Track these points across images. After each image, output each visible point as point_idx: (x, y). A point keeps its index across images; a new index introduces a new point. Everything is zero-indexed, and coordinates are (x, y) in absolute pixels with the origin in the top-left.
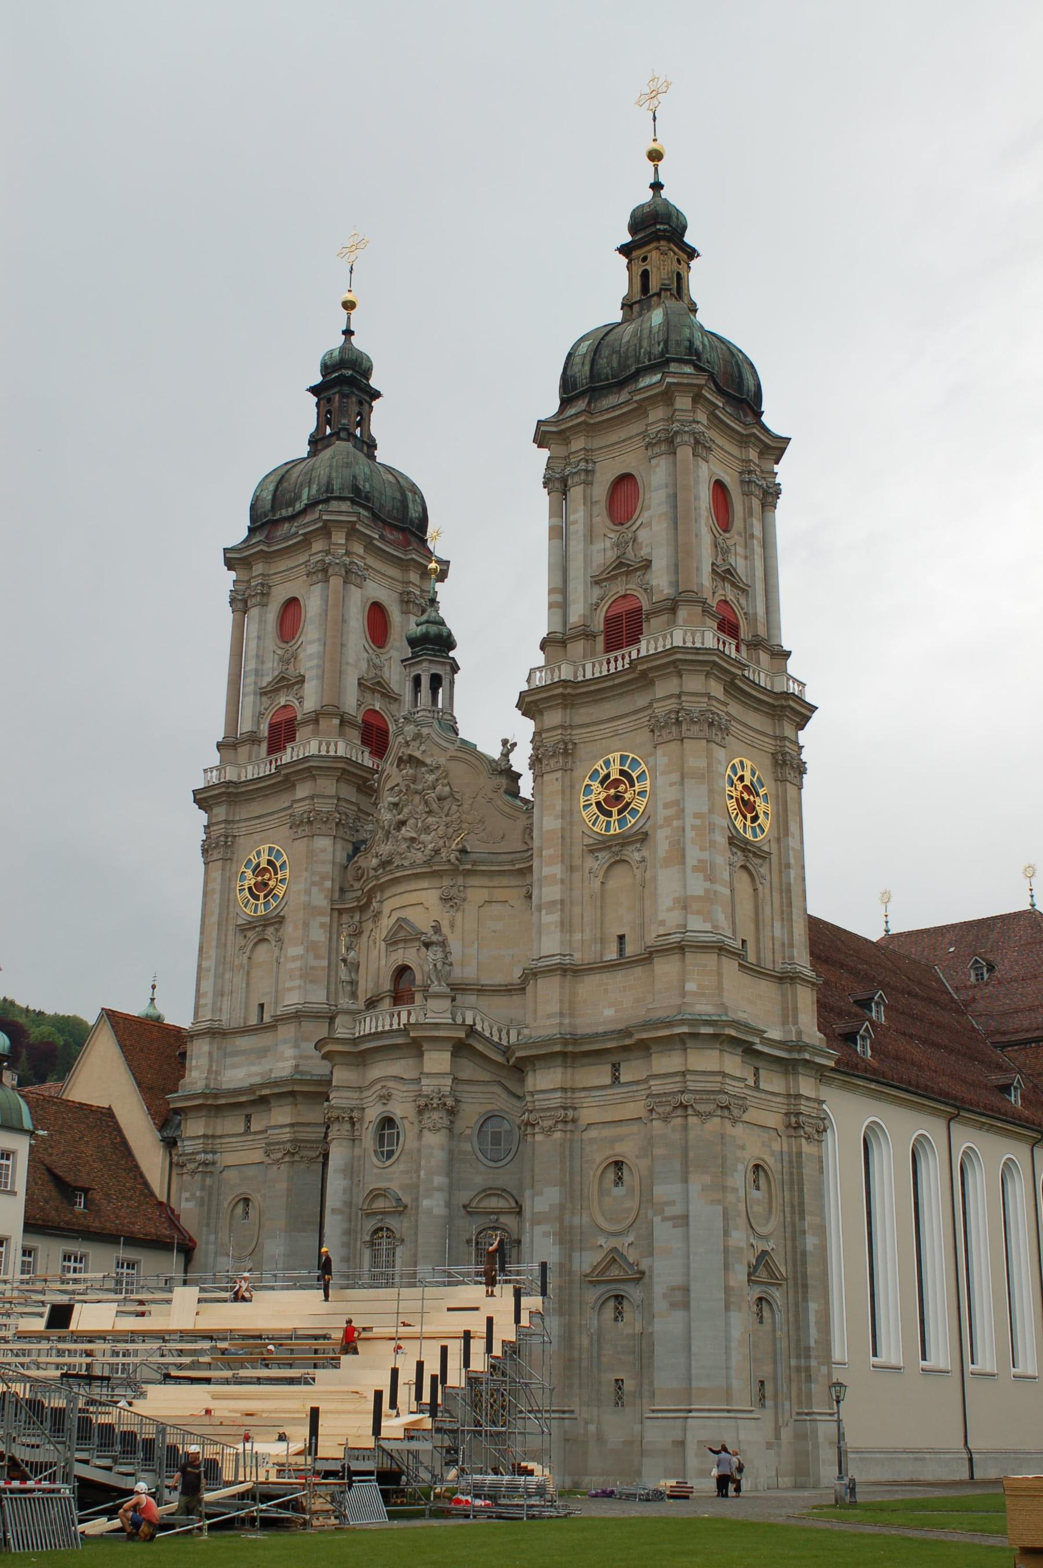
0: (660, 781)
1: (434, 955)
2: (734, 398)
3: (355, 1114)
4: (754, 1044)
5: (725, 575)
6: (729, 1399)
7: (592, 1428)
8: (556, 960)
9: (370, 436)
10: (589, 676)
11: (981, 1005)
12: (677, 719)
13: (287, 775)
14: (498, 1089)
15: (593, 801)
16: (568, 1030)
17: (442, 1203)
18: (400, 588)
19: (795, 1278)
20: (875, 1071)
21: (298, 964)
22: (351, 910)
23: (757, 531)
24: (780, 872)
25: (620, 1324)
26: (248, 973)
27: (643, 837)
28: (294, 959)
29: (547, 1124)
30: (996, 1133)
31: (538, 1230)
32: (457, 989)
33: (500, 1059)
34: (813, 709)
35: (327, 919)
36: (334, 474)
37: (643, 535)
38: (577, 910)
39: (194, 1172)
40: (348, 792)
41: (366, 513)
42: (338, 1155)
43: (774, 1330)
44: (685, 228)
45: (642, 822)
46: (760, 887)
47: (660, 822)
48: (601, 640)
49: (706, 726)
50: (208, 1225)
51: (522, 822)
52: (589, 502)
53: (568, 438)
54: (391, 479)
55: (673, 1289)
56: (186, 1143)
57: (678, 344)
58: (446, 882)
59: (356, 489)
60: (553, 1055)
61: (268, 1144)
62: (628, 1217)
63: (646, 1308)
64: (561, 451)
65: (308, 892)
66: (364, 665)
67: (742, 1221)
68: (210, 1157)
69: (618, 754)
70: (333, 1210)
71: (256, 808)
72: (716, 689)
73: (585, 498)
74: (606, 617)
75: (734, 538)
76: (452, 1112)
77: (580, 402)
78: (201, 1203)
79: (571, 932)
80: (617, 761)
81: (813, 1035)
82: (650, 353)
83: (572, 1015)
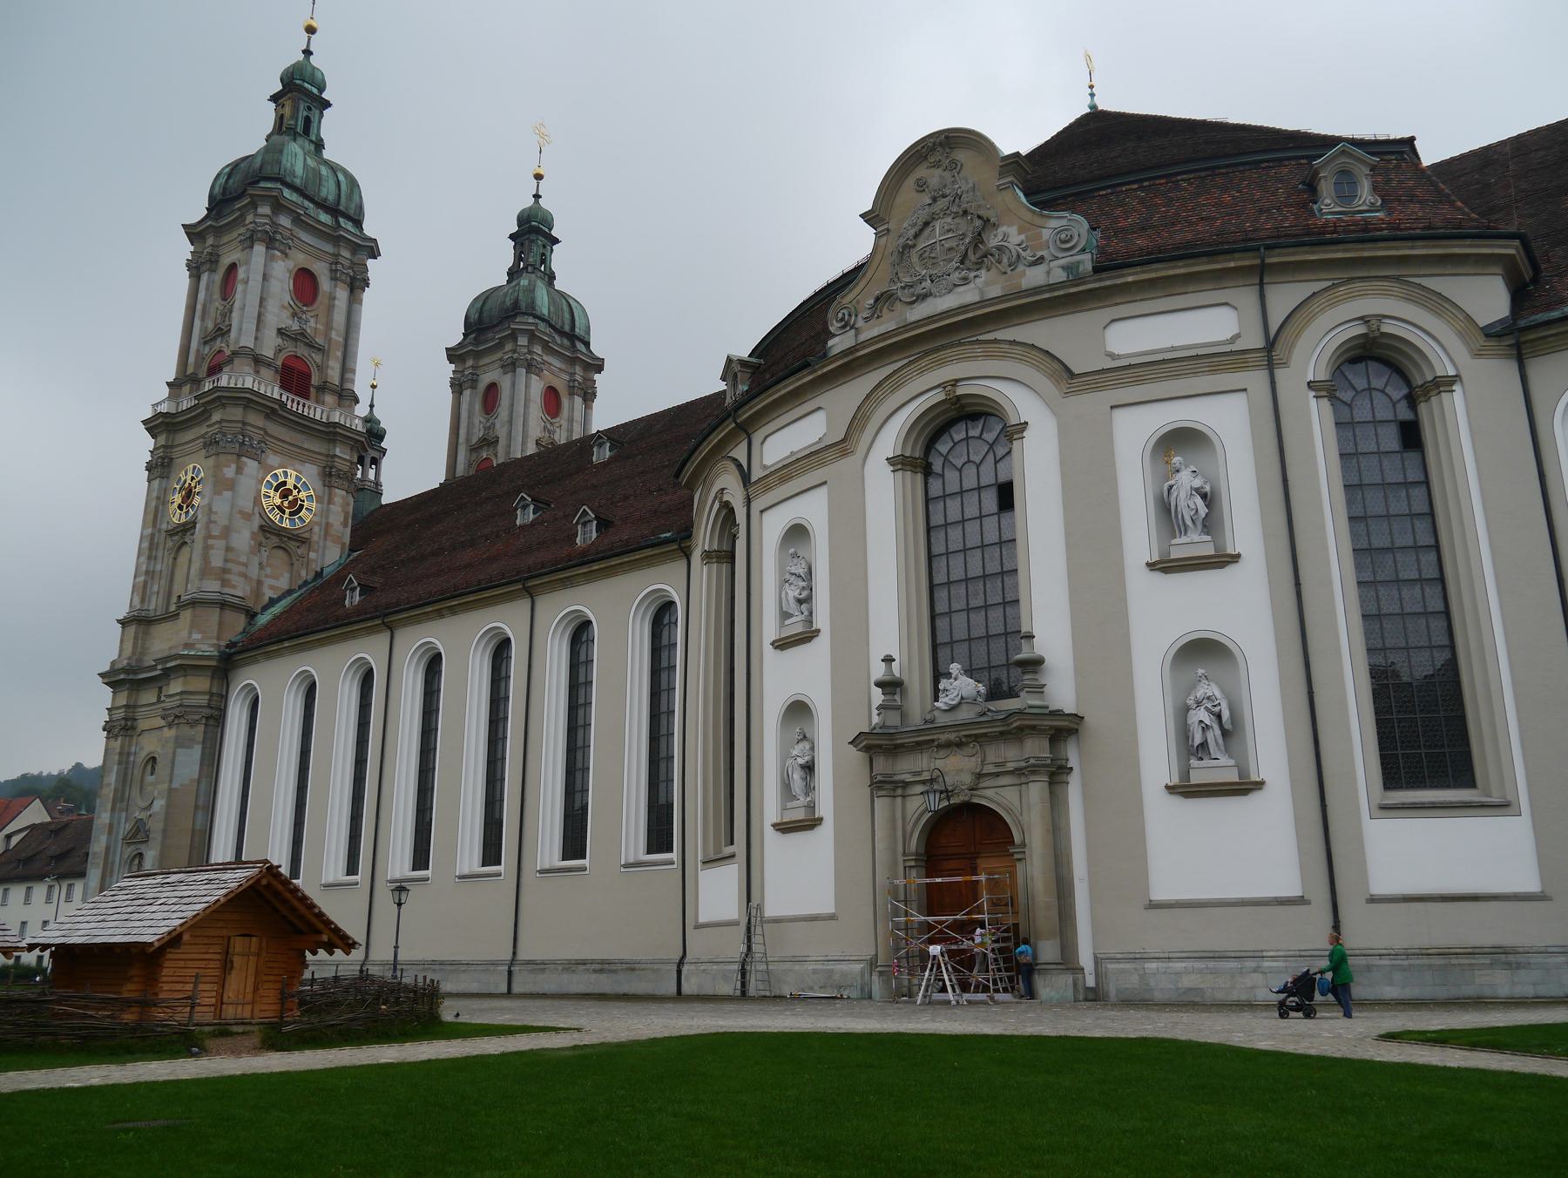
74: (208, 367)
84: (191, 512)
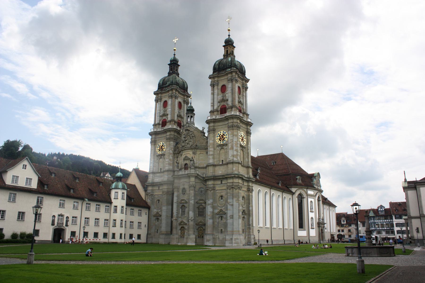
0: (230, 136)
1: (192, 162)
2: (241, 72)
3: (178, 187)
4: (243, 178)
5: (240, 102)
6: (239, 232)
7: (217, 236)
8: (212, 164)
9: (178, 73)
10: (218, 118)
11: (274, 169)
12: (232, 126)
13: (165, 131)
14: (202, 184)
16: (214, 175)
17: (193, 202)
18: (183, 99)
19: (248, 214)
20: (260, 181)
21: (167, 162)
22: (177, 153)
23: (244, 95)
24: (247, 150)
25: (222, 221)
26: (159, 163)
27: (226, 145)
28: (167, 161)
29: (210, 190)
30: (277, 191)
31: (209, 206)
32: (196, 168)
33: (202, 179)
34: (253, 124)
35: (172, 155)
36: (173, 80)
37: (227, 95)
38: (215, 156)
39: (150, 196)
40: (176, 134)
41: (178, 87)
42: (175, 194)
43: (245, 222)
44: (234, 43)
45: (226, 142)
46: (244, 153)
47: (229, 142)
48: (219, 112)
49: (237, 127)
50: (152, 204)
51: (206, 141)
52: (218, 89)
53: (214, 78)
54: (182, 81)
55: (231, 216)
56: (148, 191)
57: (233, 64)
58: (193, 150)
59: (177, 83)
60: (211, 179)
61: (163, 191)
62: (223, 204)
63: (226, 219)
64: (213, 80)
65: (169, 150)
66: (178, 112)
67: (241, 205)
68: (153, 193)
70: (175, 203)
71: (160, 136)
72: (239, 121)
73: (217, 88)
75: (241, 96)
76: (195, 187)
77: (216, 72)
78: (151, 200)
79: (214, 159)
80: (222, 132)
81: (251, 176)
82: (228, 65)
83: (214, 173)
84: (224, 142)
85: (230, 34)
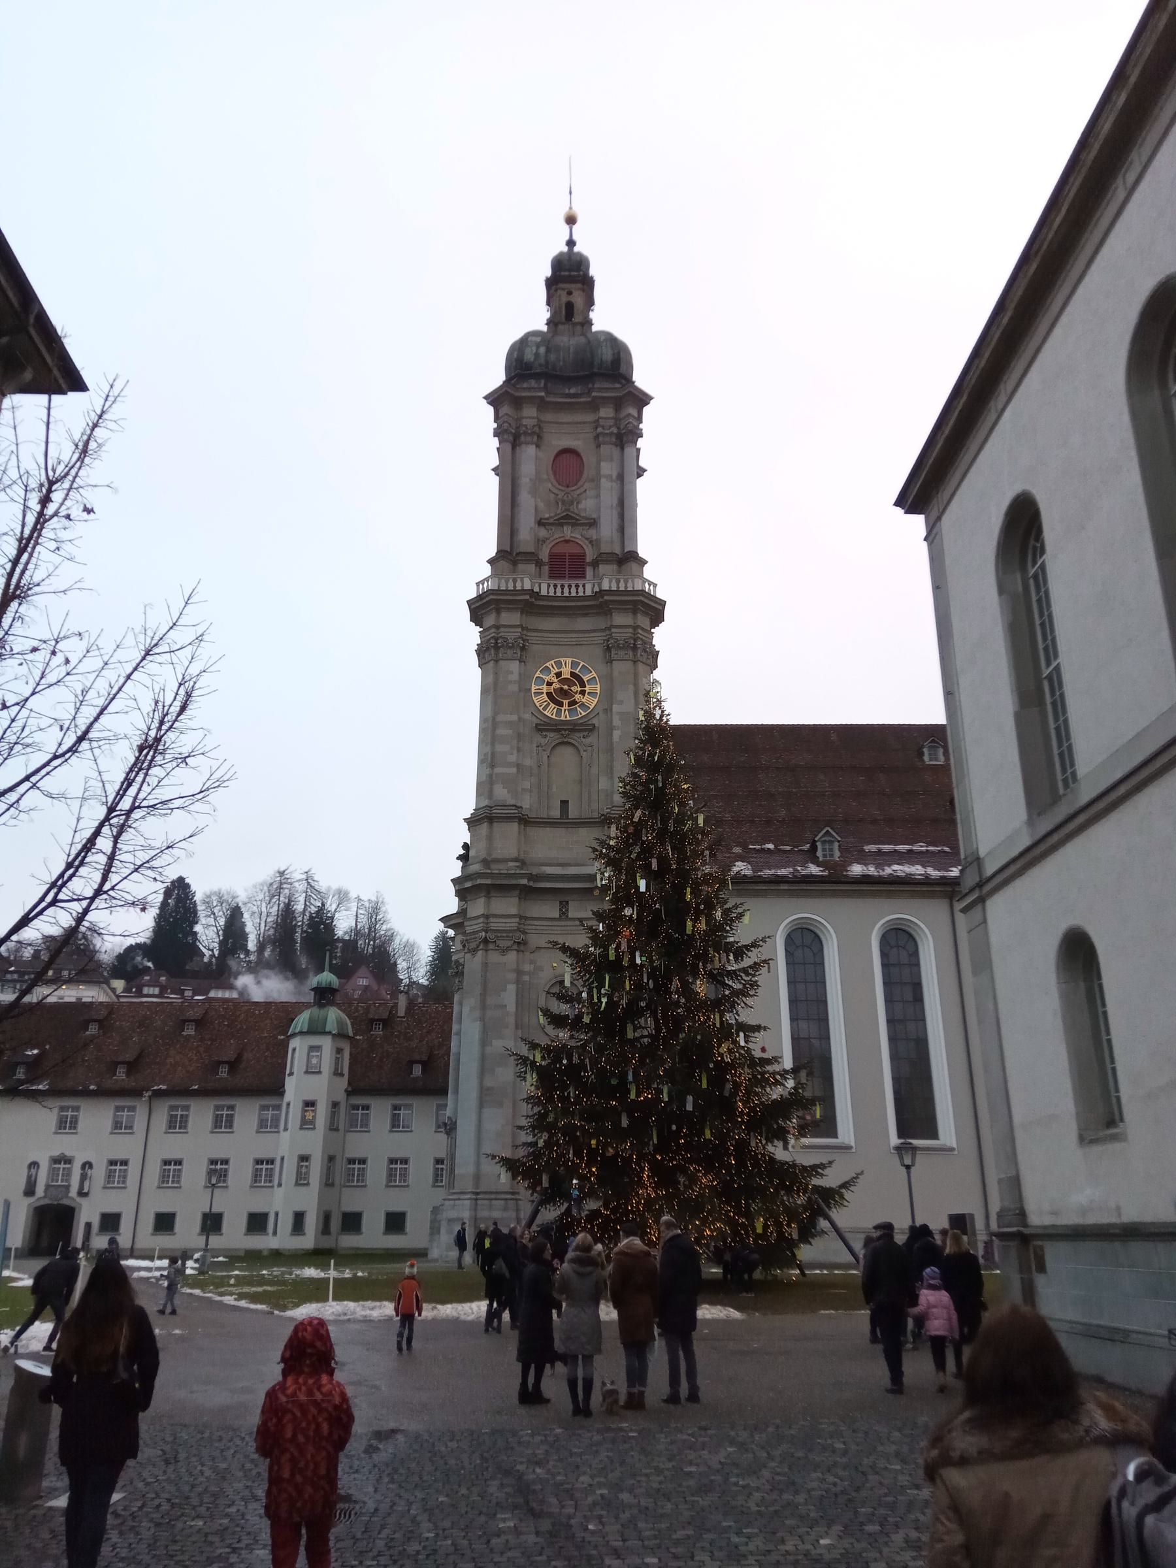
15: (545, 691)
27: (585, 728)
29: (503, 944)
69: (570, 660)
85: (575, 237)
